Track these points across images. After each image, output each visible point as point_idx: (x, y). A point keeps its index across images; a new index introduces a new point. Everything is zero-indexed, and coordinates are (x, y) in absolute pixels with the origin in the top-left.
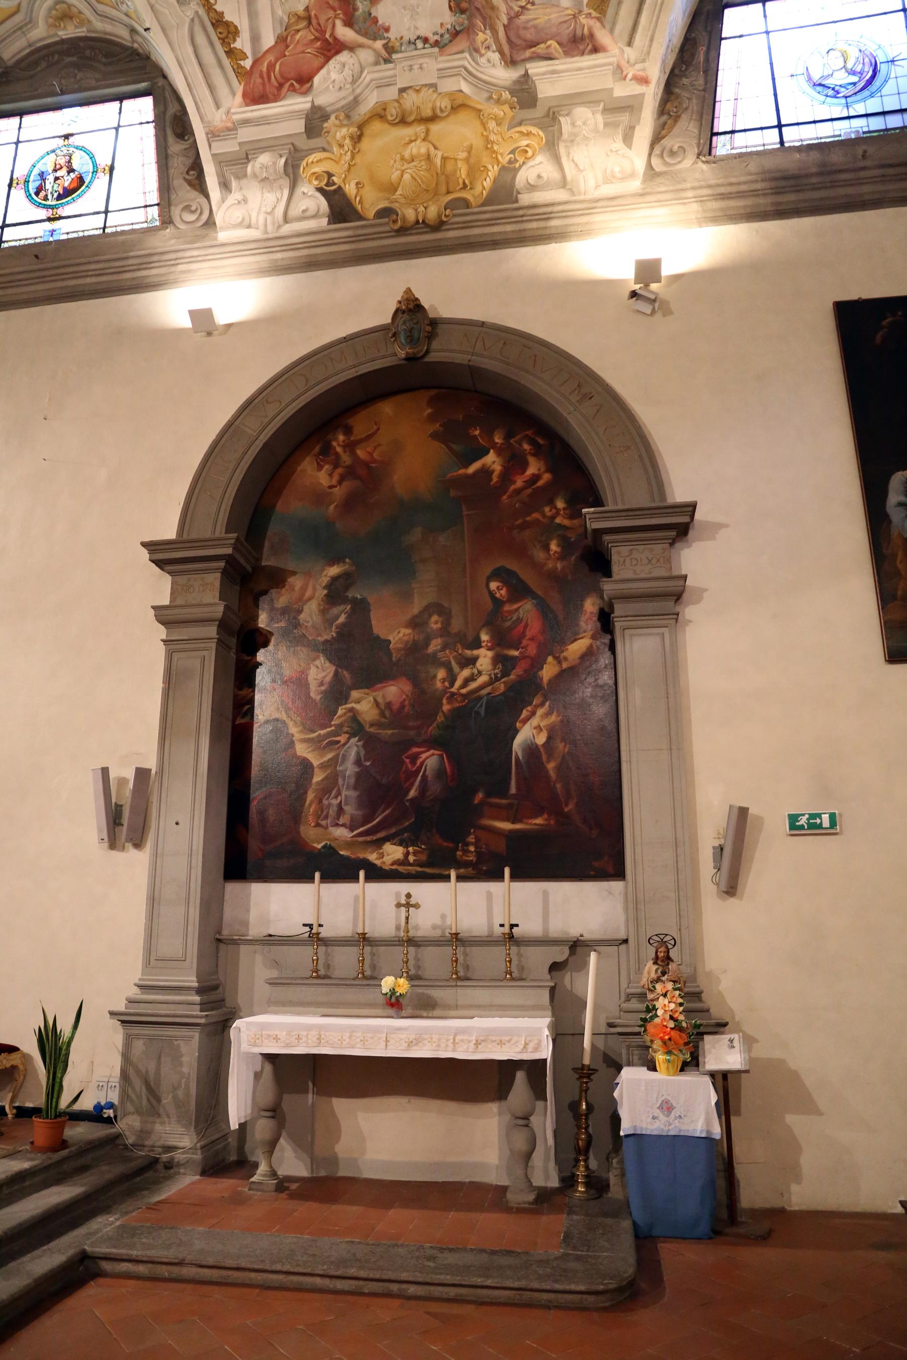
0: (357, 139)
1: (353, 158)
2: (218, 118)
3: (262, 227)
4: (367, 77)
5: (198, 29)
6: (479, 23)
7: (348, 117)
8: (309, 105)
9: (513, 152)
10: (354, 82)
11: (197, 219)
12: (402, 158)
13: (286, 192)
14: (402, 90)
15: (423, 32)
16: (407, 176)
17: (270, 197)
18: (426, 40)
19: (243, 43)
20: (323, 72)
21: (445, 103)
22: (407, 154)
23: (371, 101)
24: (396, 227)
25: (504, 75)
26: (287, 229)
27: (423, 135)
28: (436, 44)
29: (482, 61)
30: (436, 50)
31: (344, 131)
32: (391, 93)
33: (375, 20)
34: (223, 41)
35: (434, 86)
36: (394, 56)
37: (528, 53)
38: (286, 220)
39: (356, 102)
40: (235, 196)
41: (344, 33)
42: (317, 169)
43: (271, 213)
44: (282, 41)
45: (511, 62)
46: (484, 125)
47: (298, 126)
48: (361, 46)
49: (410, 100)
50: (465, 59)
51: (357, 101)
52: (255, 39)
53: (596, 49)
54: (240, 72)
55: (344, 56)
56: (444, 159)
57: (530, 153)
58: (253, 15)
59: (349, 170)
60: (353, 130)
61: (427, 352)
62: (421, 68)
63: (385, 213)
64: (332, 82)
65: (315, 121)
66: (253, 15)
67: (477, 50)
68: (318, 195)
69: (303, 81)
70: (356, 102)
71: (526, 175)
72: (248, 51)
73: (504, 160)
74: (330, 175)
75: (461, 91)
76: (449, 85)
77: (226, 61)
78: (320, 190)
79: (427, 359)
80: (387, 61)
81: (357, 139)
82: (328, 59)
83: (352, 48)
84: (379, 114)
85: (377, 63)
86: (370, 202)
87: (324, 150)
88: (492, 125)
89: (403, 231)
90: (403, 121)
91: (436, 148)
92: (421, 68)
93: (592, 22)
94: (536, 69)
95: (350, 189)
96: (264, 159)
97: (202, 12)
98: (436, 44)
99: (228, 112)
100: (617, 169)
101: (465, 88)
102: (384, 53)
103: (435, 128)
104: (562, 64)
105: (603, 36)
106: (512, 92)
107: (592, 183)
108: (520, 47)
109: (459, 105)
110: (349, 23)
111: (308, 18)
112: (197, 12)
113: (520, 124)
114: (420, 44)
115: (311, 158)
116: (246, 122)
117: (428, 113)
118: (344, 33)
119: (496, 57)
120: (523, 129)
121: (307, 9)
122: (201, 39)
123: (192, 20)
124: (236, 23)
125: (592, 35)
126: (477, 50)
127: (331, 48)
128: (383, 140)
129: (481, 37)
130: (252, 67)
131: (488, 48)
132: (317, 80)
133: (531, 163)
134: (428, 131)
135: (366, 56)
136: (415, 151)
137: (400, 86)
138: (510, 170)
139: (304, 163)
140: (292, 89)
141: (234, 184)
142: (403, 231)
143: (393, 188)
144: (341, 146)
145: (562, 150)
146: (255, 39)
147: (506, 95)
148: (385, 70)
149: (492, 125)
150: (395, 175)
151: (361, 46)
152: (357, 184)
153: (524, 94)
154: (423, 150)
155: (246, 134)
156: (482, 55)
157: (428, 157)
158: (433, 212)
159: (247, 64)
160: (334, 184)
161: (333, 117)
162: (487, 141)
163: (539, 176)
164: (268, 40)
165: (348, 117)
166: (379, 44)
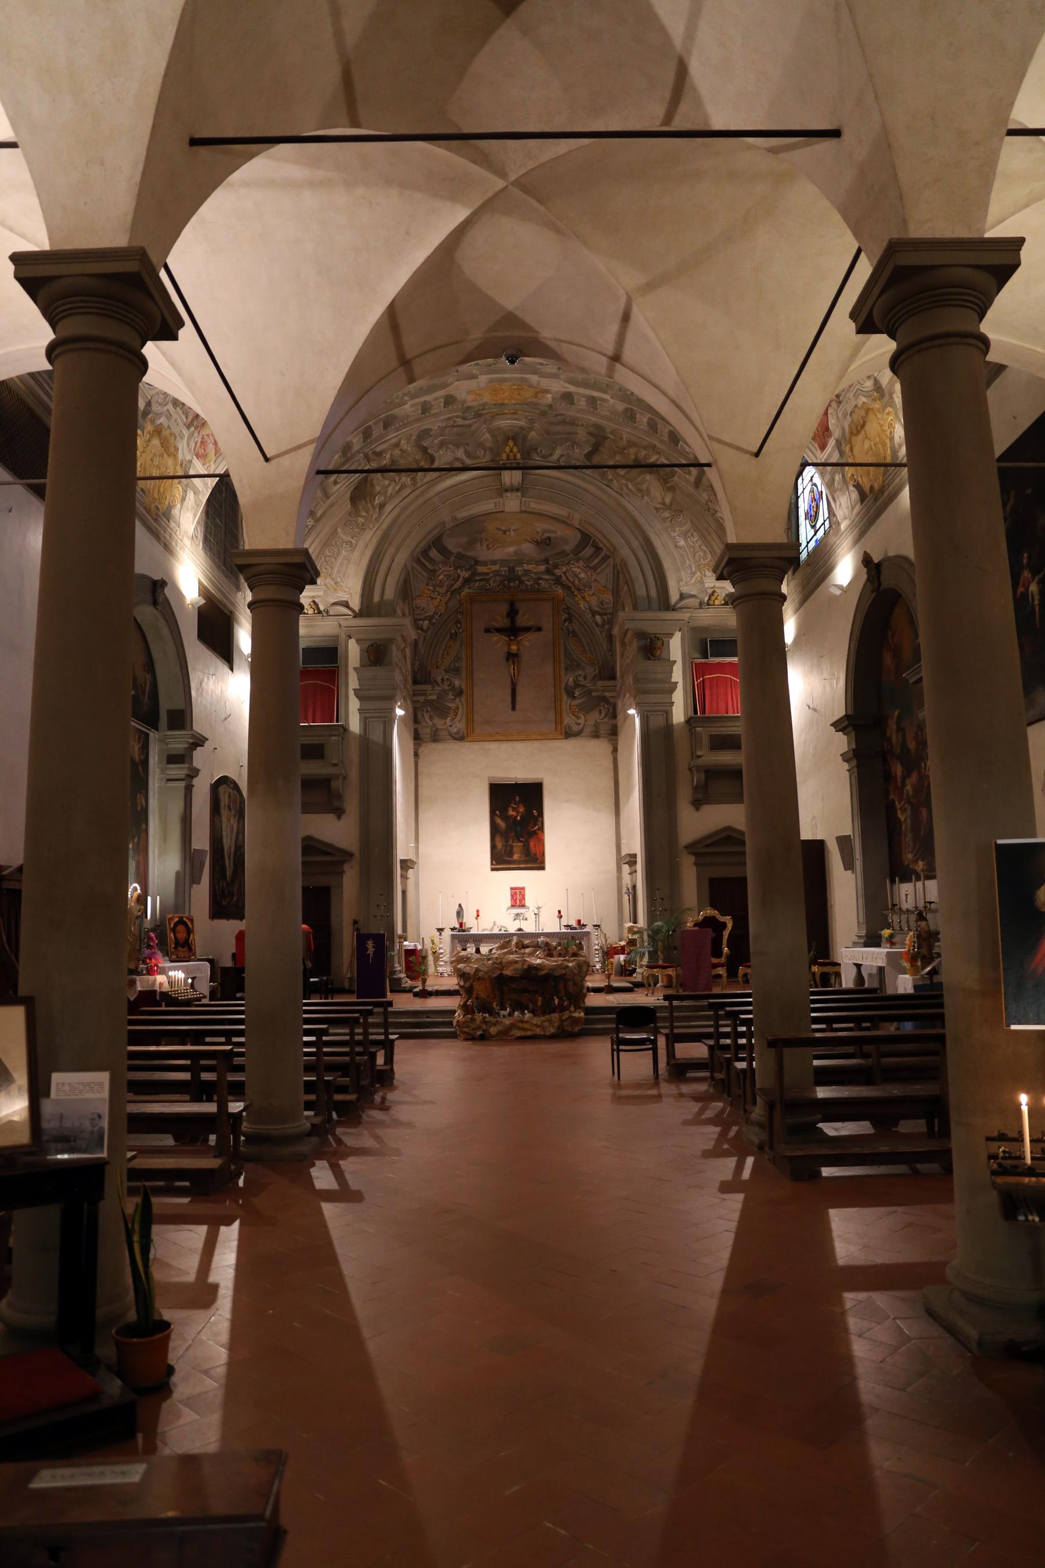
0: (851, 449)
4: (840, 415)
21: (863, 413)
61: (880, 585)
70: (844, 430)
73: (888, 433)
79: (882, 588)
80: (840, 403)
81: (851, 449)
95: (860, 480)
103: (867, 428)
117: (861, 421)
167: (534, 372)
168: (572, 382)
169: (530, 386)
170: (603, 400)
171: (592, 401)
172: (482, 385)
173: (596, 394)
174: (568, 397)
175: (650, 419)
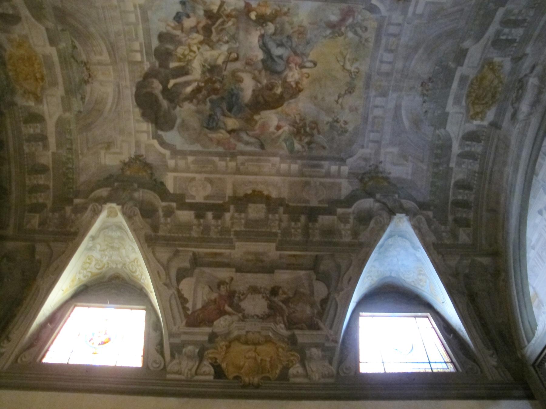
0: (228, 347)
1: (226, 353)
2: (175, 329)
3: (185, 375)
4: (235, 325)
5: (173, 297)
6: (278, 314)
7: (225, 338)
8: (211, 331)
9: (288, 361)
10: (229, 326)
11: (158, 367)
12: (245, 357)
13: (197, 364)
14: (247, 332)
15: (257, 313)
16: (247, 364)
17: (191, 364)
18: (258, 316)
19: (189, 305)
20: (218, 321)
22: (247, 356)
23: (236, 333)
24: (241, 384)
25: (285, 332)
26: (196, 378)
27: (254, 349)
28: (261, 318)
29: (278, 327)
30: (261, 320)
31: (223, 343)
32: (243, 332)
33: (240, 307)
34: (182, 303)
35: (259, 332)
36: (246, 320)
37: (295, 327)
38: (196, 374)
39: (229, 333)
40: (175, 361)
41: (228, 308)
42: (211, 356)
43: (190, 370)
44: (204, 307)
45: (288, 328)
46: (277, 349)
47: (206, 338)
48: (234, 314)
49: (250, 336)
50: (272, 325)
51: (229, 333)
52: (194, 305)
53: (319, 329)
54: (187, 316)
55: (227, 317)
56: (262, 360)
57: (294, 362)
58: (195, 298)
59: (224, 358)
60: (227, 343)
62: (255, 325)
63: (237, 378)
64: (221, 324)
65: (213, 337)
66: (195, 298)
67: (276, 323)
68: (210, 366)
69: (210, 323)
71: (292, 371)
72: (191, 308)
73: (285, 364)
74: (216, 359)
75: (269, 336)
76: (264, 333)
77: (181, 310)
78: (211, 364)
80: (243, 321)
81: (228, 347)
82: (220, 316)
83: (230, 314)
84: (238, 339)
85: (239, 321)
86: (231, 373)
87: (215, 349)
88: (280, 350)
89: (245, 386)
90: (246, 343)
91: (258, 355)
92: (255, 325)
93: (317, 320)
94: (297, 332)
95: (224, 365)
96: (190, 348)
97: (176, 293)
98: (261, 318)
99: (179, 327)
100: (327, 373)
101: (271, 334)
102: (242, 318)
103: (259, 348)
104: (307, 332)
105: (321, 325)
106: (288, 339)
107: (317, 377)
108: (291, 324)
109: (268, 340)
110: (230, 306)
111: (215, 301)
112: (174, 293)
113: (291, 351)
114: (255, 317)
115: (209, 351)
116: (185, 333)
118: (228, 308)
119: (283, 326)
120: (292, 353)
121: (215, 299)
122: (174, 302)
123: (172, 295)
124: (188, 298)
125: (317, 324)
126: (276, 323)
127: (222, 313)
128: (238, 348)
129: (278, 318)
130: (192, 314)
131: (280, 323)
132: (215, 323)
133: (294, 366)
134: (256, 349)
135: (235, 318)
136: (250, 355)
137: (247, 330)
138: (286, 369)
139: (206, 353)
140: (205, 325)
141: (177, 355)
142: (245, 386)
143: (240, 368)
144: (221, 348)
145: (306, 363)
146: (194, 305)
147: (286, 340)
148: (242, 324)
149: (280, 350)
150: (242, 363)
151: (234, 314)
152: (227, 364)
153: (292, 341)
154: (254, 355)
155: (184, 337)
156: (277, 324)
157: (255, 359)
158: (256, 380)
159: (189, 312)
160: (217, 362)
161: (219, 338)
162: (278, 355)
163: (298, 372)
164: (199, 306)
165: (225, 338)
166: (240, 315)
167: (69, 92)
168: (60, 122)
169: (43, 88)
170: (46, 147)
171: (43, 138)
172: (39, 50)
173: (52, 140)
174: (36, 118)
175: (47, 187)
